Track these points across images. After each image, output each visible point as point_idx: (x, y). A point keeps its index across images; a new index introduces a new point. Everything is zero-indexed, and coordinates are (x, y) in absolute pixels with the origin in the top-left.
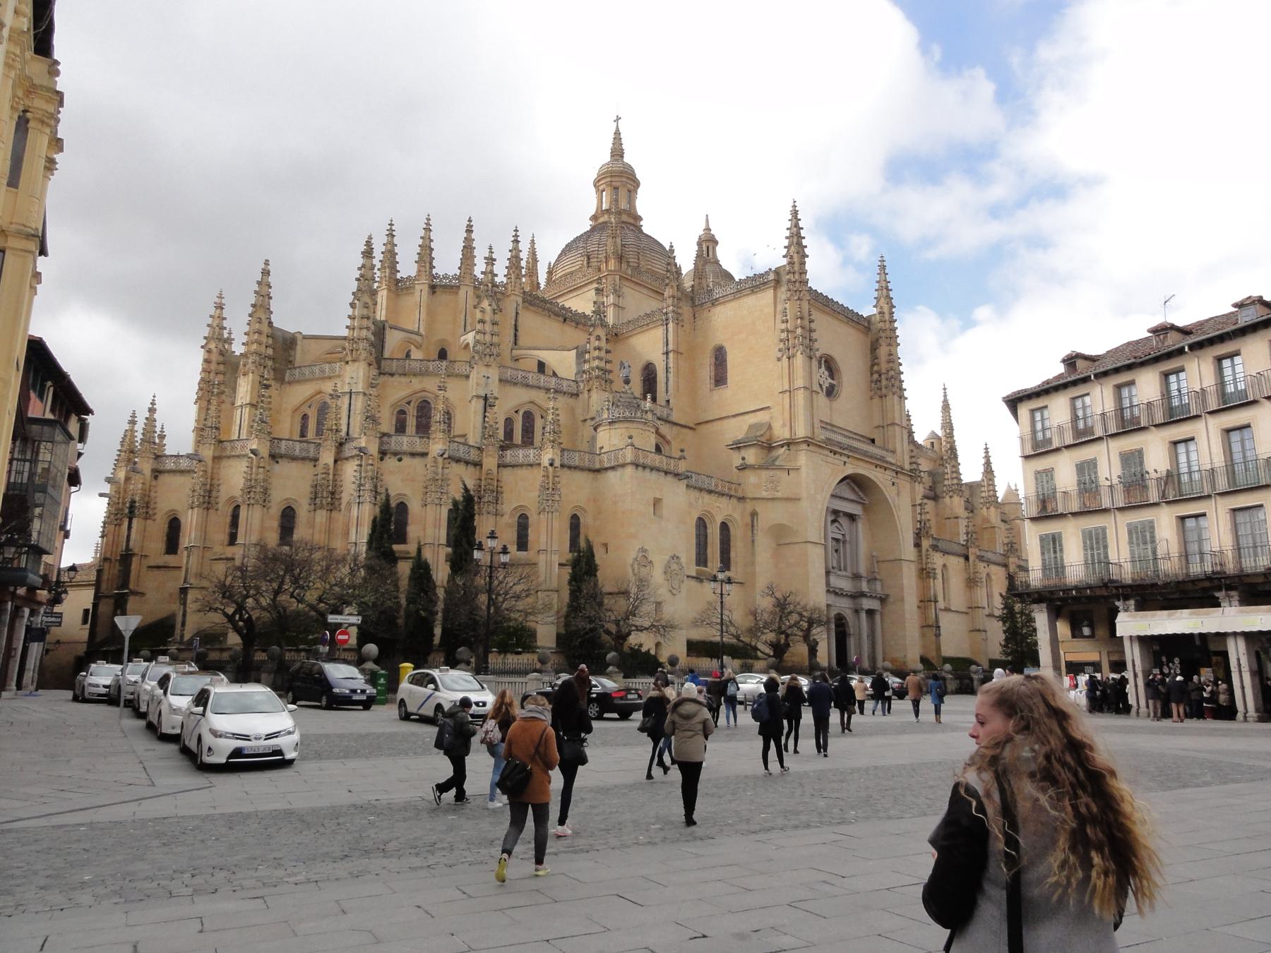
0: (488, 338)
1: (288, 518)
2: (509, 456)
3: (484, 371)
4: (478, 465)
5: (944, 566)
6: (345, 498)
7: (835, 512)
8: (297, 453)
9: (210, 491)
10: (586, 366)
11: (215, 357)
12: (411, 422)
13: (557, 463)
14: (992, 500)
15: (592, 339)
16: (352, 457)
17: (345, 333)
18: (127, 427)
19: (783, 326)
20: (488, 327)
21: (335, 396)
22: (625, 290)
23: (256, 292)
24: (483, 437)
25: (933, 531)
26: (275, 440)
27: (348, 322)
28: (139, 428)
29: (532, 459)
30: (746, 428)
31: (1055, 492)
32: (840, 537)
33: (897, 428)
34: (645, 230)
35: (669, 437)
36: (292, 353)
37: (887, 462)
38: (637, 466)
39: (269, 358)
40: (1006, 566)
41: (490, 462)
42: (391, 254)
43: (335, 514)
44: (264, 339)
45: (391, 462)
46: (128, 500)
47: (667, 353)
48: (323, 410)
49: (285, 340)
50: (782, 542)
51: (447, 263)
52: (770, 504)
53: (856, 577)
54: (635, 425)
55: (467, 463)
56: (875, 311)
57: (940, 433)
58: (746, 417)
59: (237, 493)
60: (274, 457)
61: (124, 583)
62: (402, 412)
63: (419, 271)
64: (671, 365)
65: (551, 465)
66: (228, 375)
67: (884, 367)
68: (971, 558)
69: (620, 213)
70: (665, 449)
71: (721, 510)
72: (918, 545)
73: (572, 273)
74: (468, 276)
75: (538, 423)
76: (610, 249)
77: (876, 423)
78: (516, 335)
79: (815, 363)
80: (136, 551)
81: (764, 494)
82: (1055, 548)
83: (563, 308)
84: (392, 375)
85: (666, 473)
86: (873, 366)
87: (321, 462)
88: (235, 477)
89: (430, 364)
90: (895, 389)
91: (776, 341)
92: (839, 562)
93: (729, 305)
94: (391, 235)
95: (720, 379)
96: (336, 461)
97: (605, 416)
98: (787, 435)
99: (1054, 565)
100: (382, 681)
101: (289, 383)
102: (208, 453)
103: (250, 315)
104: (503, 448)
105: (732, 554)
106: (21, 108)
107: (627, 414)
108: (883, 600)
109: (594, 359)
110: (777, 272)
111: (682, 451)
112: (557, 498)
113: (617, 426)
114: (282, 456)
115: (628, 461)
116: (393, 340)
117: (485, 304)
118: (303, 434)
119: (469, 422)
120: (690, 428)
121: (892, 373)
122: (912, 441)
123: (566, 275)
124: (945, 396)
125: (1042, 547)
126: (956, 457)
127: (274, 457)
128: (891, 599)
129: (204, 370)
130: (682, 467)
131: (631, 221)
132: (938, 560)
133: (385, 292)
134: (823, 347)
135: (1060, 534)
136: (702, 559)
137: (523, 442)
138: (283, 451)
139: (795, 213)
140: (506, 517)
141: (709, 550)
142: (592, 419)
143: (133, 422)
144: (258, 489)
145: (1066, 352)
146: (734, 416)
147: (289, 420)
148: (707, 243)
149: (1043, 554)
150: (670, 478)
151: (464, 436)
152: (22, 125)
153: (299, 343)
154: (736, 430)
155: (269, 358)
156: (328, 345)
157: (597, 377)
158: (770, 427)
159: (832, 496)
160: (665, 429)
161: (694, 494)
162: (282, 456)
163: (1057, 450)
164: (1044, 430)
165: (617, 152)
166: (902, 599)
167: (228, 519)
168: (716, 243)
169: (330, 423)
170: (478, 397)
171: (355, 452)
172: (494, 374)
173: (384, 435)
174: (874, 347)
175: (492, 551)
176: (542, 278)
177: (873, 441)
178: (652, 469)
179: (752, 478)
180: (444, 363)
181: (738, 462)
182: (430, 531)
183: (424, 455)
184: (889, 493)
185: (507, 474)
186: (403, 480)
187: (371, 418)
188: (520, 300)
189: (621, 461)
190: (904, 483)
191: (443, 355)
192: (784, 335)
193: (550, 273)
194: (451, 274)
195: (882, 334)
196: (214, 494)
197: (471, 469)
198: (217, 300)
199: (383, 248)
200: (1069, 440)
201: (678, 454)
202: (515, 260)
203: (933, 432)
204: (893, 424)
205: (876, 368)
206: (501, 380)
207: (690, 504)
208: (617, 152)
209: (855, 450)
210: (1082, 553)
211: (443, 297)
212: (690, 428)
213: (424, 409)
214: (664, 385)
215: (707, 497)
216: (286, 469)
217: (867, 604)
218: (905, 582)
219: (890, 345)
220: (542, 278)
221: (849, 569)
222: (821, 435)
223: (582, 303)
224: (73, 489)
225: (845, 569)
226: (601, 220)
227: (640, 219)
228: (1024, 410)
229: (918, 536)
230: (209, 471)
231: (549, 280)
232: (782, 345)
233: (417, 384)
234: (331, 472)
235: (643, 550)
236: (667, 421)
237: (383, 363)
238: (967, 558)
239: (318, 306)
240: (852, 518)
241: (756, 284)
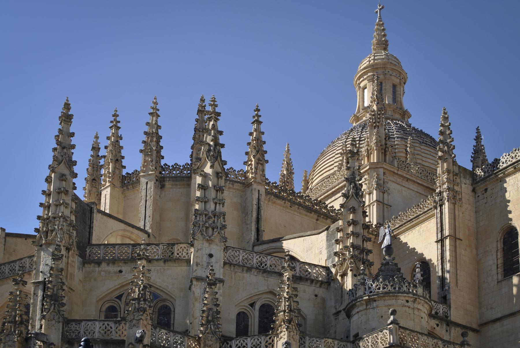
3: (207, 249)
51: (177, 152)
78: (258, 230)
84: (98, 263)
109: (348, 236)
117: (208, 170)
133: (109, 189)
194: (182, 163)
211: (172, 190)
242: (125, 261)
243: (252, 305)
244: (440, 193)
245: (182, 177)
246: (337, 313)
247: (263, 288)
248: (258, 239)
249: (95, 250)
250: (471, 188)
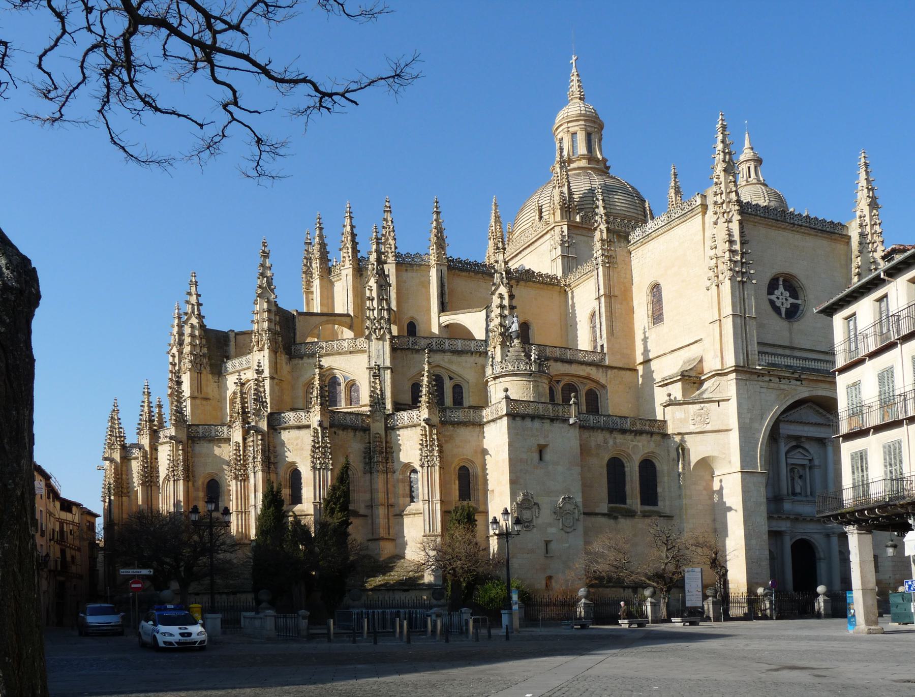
4: (366, 430)
29: (415, 421)
30: (681, 363)
35: (603, 381)
55: (355, 429)
76: (557, 199)
82: (862, 466)
85: (552, 420)
96: (244, 439)
99: (862, 485)
125: (853, 466)
138: (201, 435)
146: (673, 351)
149: (853, 473)
150: (557, 425)
158: (701, 361)
178: (533, 417)
183: (308, 427)
197: (359, 434)
210: (883, 467)
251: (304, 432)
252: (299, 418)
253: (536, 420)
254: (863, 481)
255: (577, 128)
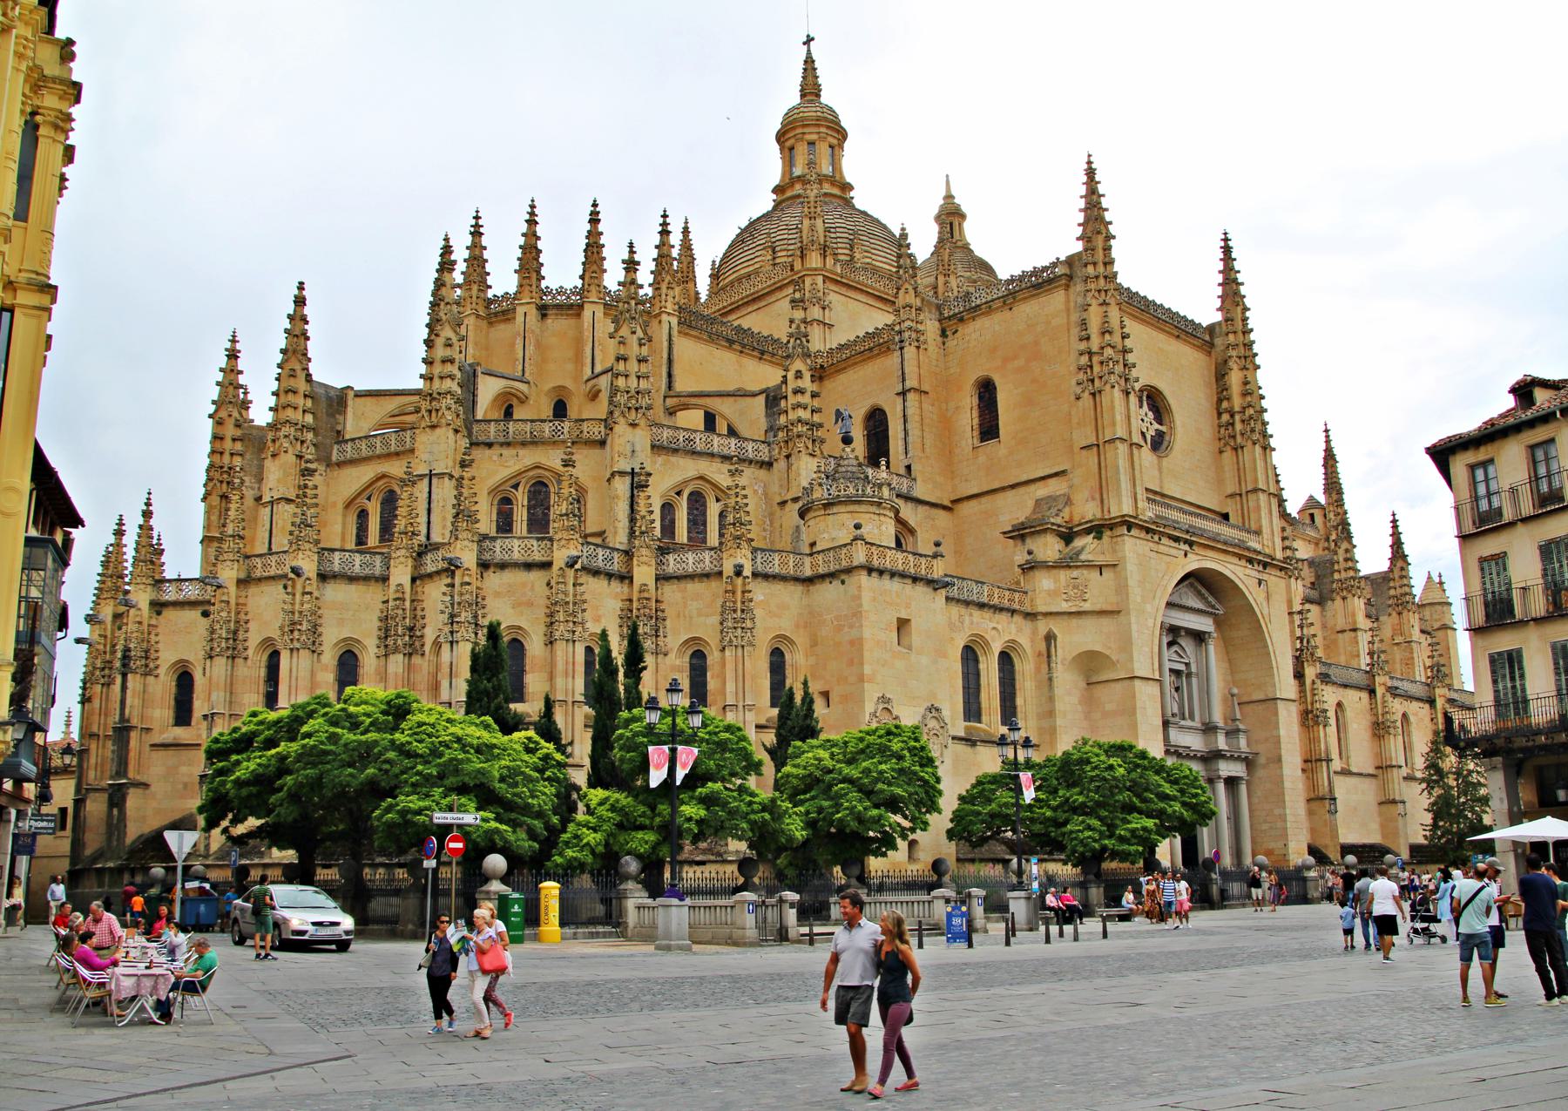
0: (633, 383)
1: (348, 668)
2: (672, 564)
4: (626, 578)
5: (1339, 705)
6: (430, 635)
7: (1174, 632)
8: (357, 569)
9: (235, 632)
10: (783, 420)
11: (230, 431)
12: (521, 516)
13: (747, 572)
14: (1403, 602)
15: (790, 375)
16: (438, 573)
17: (419, 384)
18: (112, 539)
19: (1083, 346)
20: (633, 366)
21: (410, 480)
22: (833, 297)
23: (286, 331)
24: (632, 533)
25: (1319, 653)
26: (324, 552)
27: (423, 369)
28: (130, 539)
30: (1031, 504)
31: (1509, 590)
32: (1182, 667)
33: (1262, 497)
34: (859, 203)
35: (912, 522)
36: (341, 418)
37: (1248, 549)
38: (870, 570)
39: (309, 429)
40: (1431, 702)
41: (644, 573)
42: (477, 260)
43: (416, 660)
44: (300, 401)
45: (494, 580)
46: (119, 647)
47: (903, 393)
48: (390, 501)
49: (329, 399)
50: (1094, 679)
52: (1074, 622)
53: (1209, 729)
54: (863, 508)
55: (610, 576)
56: (1218, 317)
57: (1322, 499)
58: (1032, 488)
59: (275, 634)
60: (323, 577)
61: (122, 769)
62: (507, 501)
63: (521, 286)
64: (909, 412)
65: (738, 573)
66: (248, 456)
67: (1237, 402)
68: (1380, 691)
69: (822, 178)
70: (908, 543)
71: (999, 632)
72: (1299, 675)
73: (748, 276)
74: (593, 288)
75: (713, 509)
77: (1231, 488)
78: (670, 375)
79: (1133, 399)
80: (134, 722)
81: (1065, 607)
83: (739, 329)
84: (490, 445)
85: (915, 579)
86: (1220, 401)
87: (393, 581)
88: (266, 611)
89: (547, 427)
90: (1256, 437)
91: (1073, 368)
92: (1181, 707)
93: (997, 317)
94: (476, 233)
95: (989, 429)
96: (413, 580)
97: (817, 494)
98: (1099, 515)
99: (1512, 701)
100: (516, 908)
101: (339, 464)
102: (229, 574)
103: (279, 366)
104: (663, 551)
105: (1019, 701)
106: (29, 110)
107: (851, 491)
108: (1249, 762)
110: (1070, 261)
111: (937, 544)
112: (749, 624)
113: (835, 510)
114: (335, 576)
115: (855, 563)
116: (488, 389)
118: (361, 539)
119: (609, 512)
120: (945, 508)
121: (1251, 411)
122: (1284, 515)
123: (739, 280)
124: (1328, 441)
125: (1493, 672)
126: (1349, 537)
127: (323, 577)
128: (1262, 760)
129: (213, 452)
130: (938, 570)
131: (836, 191)
132: (1329, 696)
134: (1144, 375)
135: (1519, 651)
136: (972, 710)
137: (690, 539)
138: (336, 568)
139: (1090, 172)
140: (672, 656)
141: (983, 695)
142: (795, 500)
143: (119, 533)
144: (304, 628)
145: (1515, 377)
146: (1013, 487)
147: (340, 519)
148: (950, 217)
149: (1495, 682)
150: (921, 589)
151: (601, 534)
152: (31, 130)
153: (350, 403)
154: (1016, 508)
155: (309, 429)
156: (392, 404)
157: (799, 436)
158: (1068, 501)
159: (1170, 605)
160: (907, 511)
161: (955, 610)
162: (335, 576)
163: (1511, 524)
164: (1489, 495)
165: (810, 87)
166: (1279, 760)
167: (263, 672)
168: (963, 216)
169: (401, 524)
170: (622, 473)
171: (442, 565)
172: (641, 438)
173: (485, 537)
174: (1221, 375)
175: (673, 713)
176: (703, 284)
177: (1226, 517)
178: (893, 574)
179: (1044, 582)
180: (567, 425)
181: (1021, 557)
182: (560, 682)
183: (547, 565)
184: (1255, 595)
185: (670, 592)
186: (512, 604)
187: (462, 514)
188: (674, 321)
189: (844, 563)
190: (1274, 579)
191: (560, 410)
192: (1084, 360)
193: (715, 276)
194: (569, 285)
195: (1234, 353)
196: (241, 636)
198: (228, 345)
199: (466, 254)
200: (1527, 508)
201: (930, 550)
202: (662, 259)
203: (1311, 498)
204: (1256, 490)
205: (1225, 405)
206: (653, 447)
207: (951, 626)
208: (810, 87)
209: (1201, 533)
211: (556, 324)
212: (945, 508)
213: (539, 493)
214: (901, 443)
215: (977, 614)
216: (335, 593)
217: (1226, 769)
218: (1282, 732)
219: (1245, 368)
220: (703, 284)
221: (1197, 717)
222: (1148, 512)
223: (773, 321)
224: (60, 635)
225: (1192, 717)
226: (789, 194)
227: (849, 187)
228: (1459, 465)
229: (1299, 663)
230: (233, 602)
231: (715, 291)
232: (1081, 376)
233: (528, 457)
234: (408, 596)
235: (884, 699)
236: (908, 498)
237: (475, 428)
238: (1372, 692)
239: (377, 347)
240: (1199, 637)
241: (1037, 283)
242: (524, 444)
243: (678, 493)
244: (900, 332)
245: (571, 307)
246: (783, 504)
247: (692, 473)
248: (670, 387)
249: (483, 426)
250: (937, 324)
251: (536, 576)
252: (528, 549)
253: (896, 579)
254: (1514, 694)
255: (814, 137)
